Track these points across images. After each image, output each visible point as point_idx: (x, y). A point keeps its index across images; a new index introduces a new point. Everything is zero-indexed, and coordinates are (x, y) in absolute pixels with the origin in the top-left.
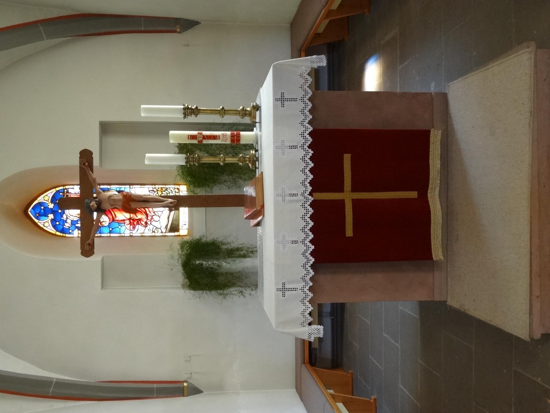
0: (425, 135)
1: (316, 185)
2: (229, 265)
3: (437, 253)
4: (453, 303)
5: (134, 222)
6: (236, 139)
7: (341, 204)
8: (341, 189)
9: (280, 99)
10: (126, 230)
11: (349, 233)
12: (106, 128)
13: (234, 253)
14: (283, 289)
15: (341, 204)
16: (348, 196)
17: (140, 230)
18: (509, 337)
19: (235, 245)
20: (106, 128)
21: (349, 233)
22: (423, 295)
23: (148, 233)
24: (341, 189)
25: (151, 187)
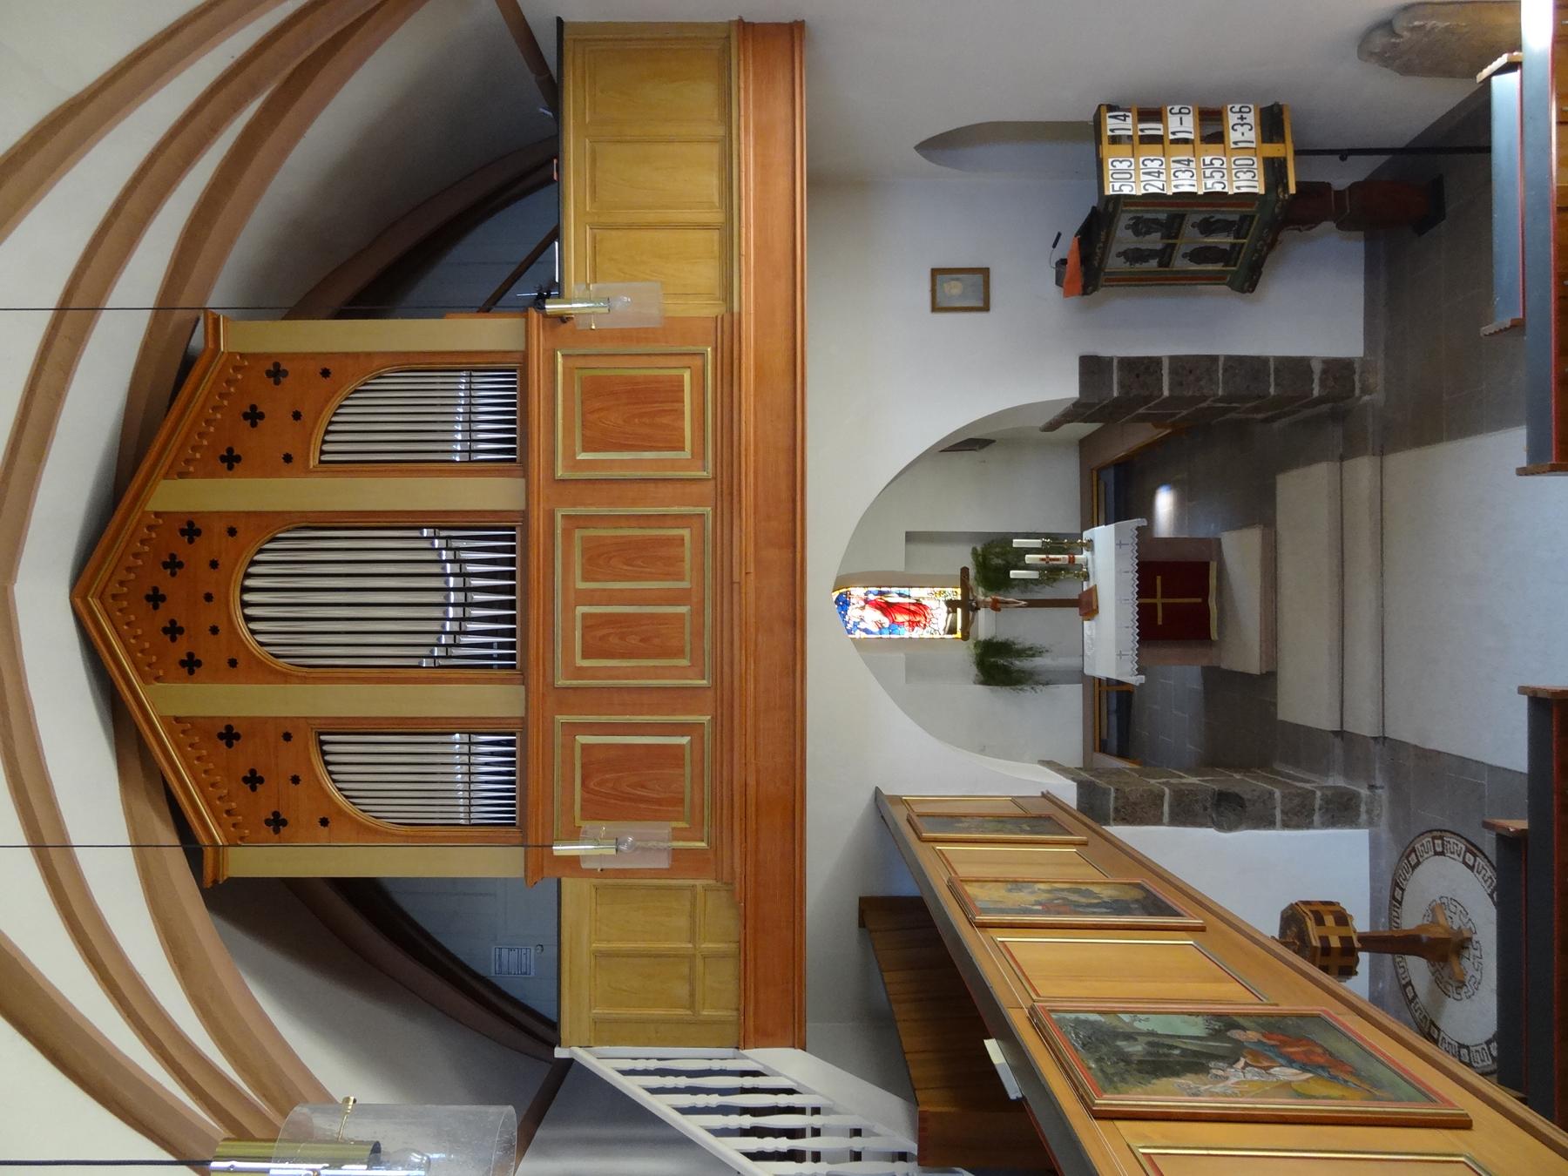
0: (1206, 565)
1: (1140, 594)
2: (1019, 664)
3: (1214, 635)
4: (1224, 666)
5: (913, 624)
6: (1072, 561)
7: (1155, 605)
8: (1154, 596)
9: (1119, 544)
10: (905, 632)
11: (1160, 622)
12: (910, 537)
13: (1032, 652)
14: (1120, 655)
15: (1155, 605)
16: (1159, 601)
17: (918, 633)
18: (1250, 676)
19: (1028, 644)
20: (910, 537)
21: (1160, 622)
22: (1205, 662)
23: (926, 635)
24: (1154, 596)
25: (929, 590)
